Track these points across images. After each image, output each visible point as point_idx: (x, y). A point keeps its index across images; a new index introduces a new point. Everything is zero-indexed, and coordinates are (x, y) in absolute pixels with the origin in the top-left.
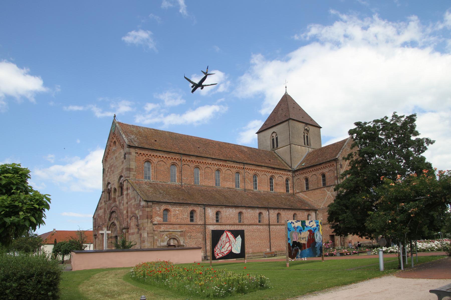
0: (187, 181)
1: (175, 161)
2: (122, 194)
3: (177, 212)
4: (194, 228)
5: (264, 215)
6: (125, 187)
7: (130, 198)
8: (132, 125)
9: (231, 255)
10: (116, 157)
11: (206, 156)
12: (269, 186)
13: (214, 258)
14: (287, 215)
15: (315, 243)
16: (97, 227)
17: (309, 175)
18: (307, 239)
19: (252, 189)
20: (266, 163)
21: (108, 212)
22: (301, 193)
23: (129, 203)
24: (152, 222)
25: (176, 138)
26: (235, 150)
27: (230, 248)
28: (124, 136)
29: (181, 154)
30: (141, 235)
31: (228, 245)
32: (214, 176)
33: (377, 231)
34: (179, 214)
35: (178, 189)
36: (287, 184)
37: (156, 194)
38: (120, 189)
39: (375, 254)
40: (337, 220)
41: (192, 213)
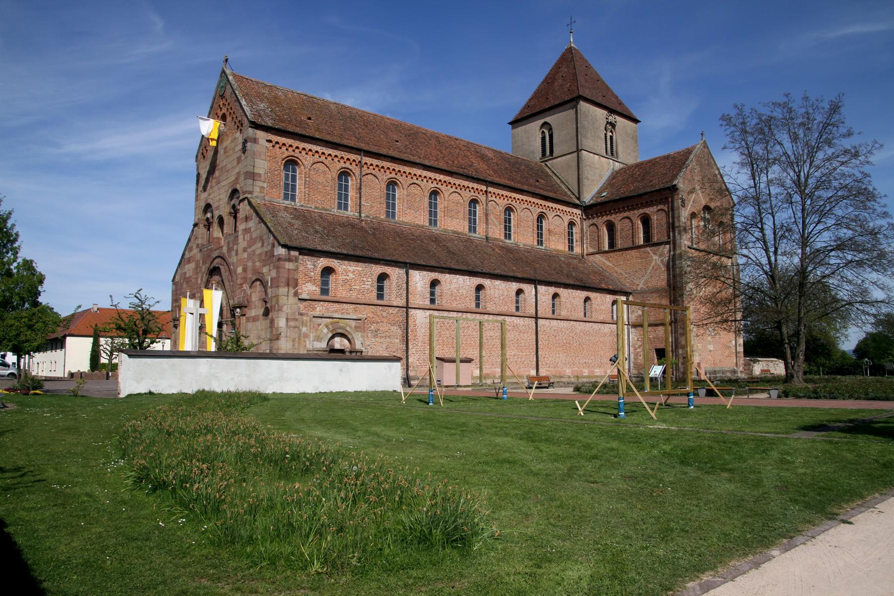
1: (347, 165)
4: (385, 314)
5: (526, 292)
6: (241, 215)
11: (412, 159)
17: (615, 218)
19: (503, 238)
24: (296, 294)
25: (350, 117)
26: (468, 154)
34: (354, 277)
35: (353, 226)
36: (570, 234)
41: (383, 277)
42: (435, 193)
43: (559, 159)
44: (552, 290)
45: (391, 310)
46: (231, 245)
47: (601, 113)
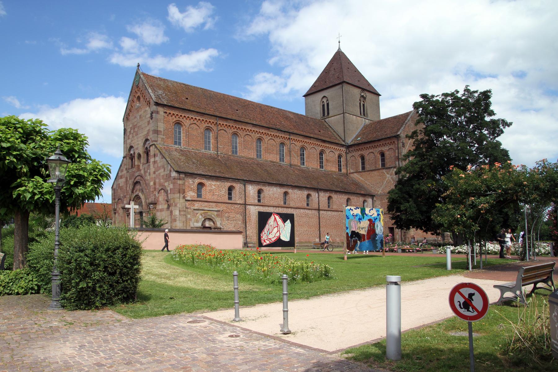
0: (225, 150)
1: (209, 125)
2: (148, 161)
3: (214, 187)
4: (233, 208)
5: (313, 197)
6: (152, 153)
7: (158, 167)
8: (159, 78)
9: (279, 243)
10: (140, 116)
12: (319, 163)
13: (260, 245)
14: (339, 199)
15: (376, 235)
16: (117, 200)
17: (365, 153)
18: (366, 229)
19: (299, 164)
20: (316, 134)
21: (131, 182)
22: (355, 174)
23: (156, 173)
24: (184, 197)
25: (210, 97)
27: (278, 235)
28: (150, 91)
29: (216, 116)
30: (171, 212)
31: (276, 230)
32: (255, 146)
33: (446, 226)
34: (215, 189)
35: (214, 159)
36: (340, 162)
37: (188, 163)
38: (146, 155)
39: (441, 253)
40: (398, 210)
41: (230, 189)
42: (260, 140)
43: (333, 118)
44: (327, 195)
45: (236, 206)
46: (146, 170)
47: (357, 92)
